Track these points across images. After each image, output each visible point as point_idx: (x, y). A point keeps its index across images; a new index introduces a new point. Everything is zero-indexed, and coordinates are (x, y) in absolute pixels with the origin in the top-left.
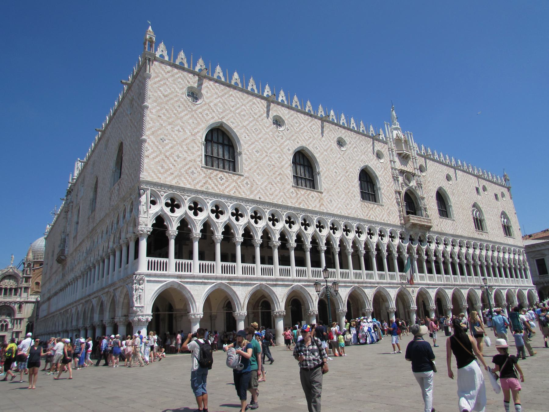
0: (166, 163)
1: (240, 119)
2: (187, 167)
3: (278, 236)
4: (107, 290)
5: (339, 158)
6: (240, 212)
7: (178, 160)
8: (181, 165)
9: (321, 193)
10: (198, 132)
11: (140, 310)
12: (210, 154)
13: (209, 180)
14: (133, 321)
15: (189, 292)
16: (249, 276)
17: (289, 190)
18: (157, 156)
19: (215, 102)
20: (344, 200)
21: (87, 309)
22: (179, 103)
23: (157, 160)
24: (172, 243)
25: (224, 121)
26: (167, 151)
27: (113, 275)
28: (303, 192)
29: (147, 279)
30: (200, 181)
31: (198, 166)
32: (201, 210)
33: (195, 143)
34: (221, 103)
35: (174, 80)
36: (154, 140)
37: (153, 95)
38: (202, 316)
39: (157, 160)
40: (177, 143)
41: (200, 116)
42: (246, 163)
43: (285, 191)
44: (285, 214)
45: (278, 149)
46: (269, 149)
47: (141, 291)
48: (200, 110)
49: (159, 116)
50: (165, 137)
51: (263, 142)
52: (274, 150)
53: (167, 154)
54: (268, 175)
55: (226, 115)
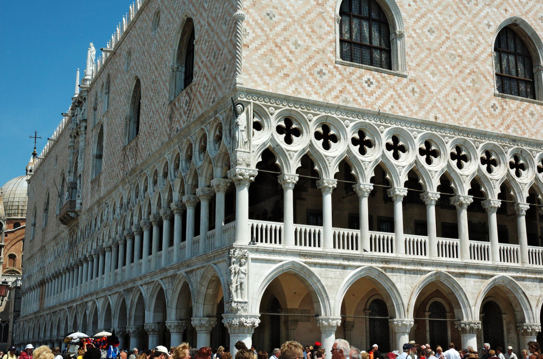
0: (276, 56)
3: (467, 187)
4: (171, 272)
6: (367, 138)
7: (297, 51)
8: (301, 60)
11: (242, 307)
12: (347, 37)
14: (231, 325)
15: (319, 281)
16: (416, 256)
17: (489, 101)
18: (262, 44)
21: (128, 303)
23: (261, 52)
24: (289, 196)
26: (278, 35)
27: (182, 248)
29: (252, 256)
30: (334, 88)
31: (330, 60)
32: (335, 139)
33: (324, 18)
36: (257, 17)
38: (340, 322)
39: (261, 52)
40: (294, 21)
43: (482, 103)
44: (481, 145)
45: (470, 25)
46: (451, 26)
47: (243, 275)
50: (275, 11)
51: (440, 13)
52: (462, 27)
53: (279, 41)
54: (450, 75)
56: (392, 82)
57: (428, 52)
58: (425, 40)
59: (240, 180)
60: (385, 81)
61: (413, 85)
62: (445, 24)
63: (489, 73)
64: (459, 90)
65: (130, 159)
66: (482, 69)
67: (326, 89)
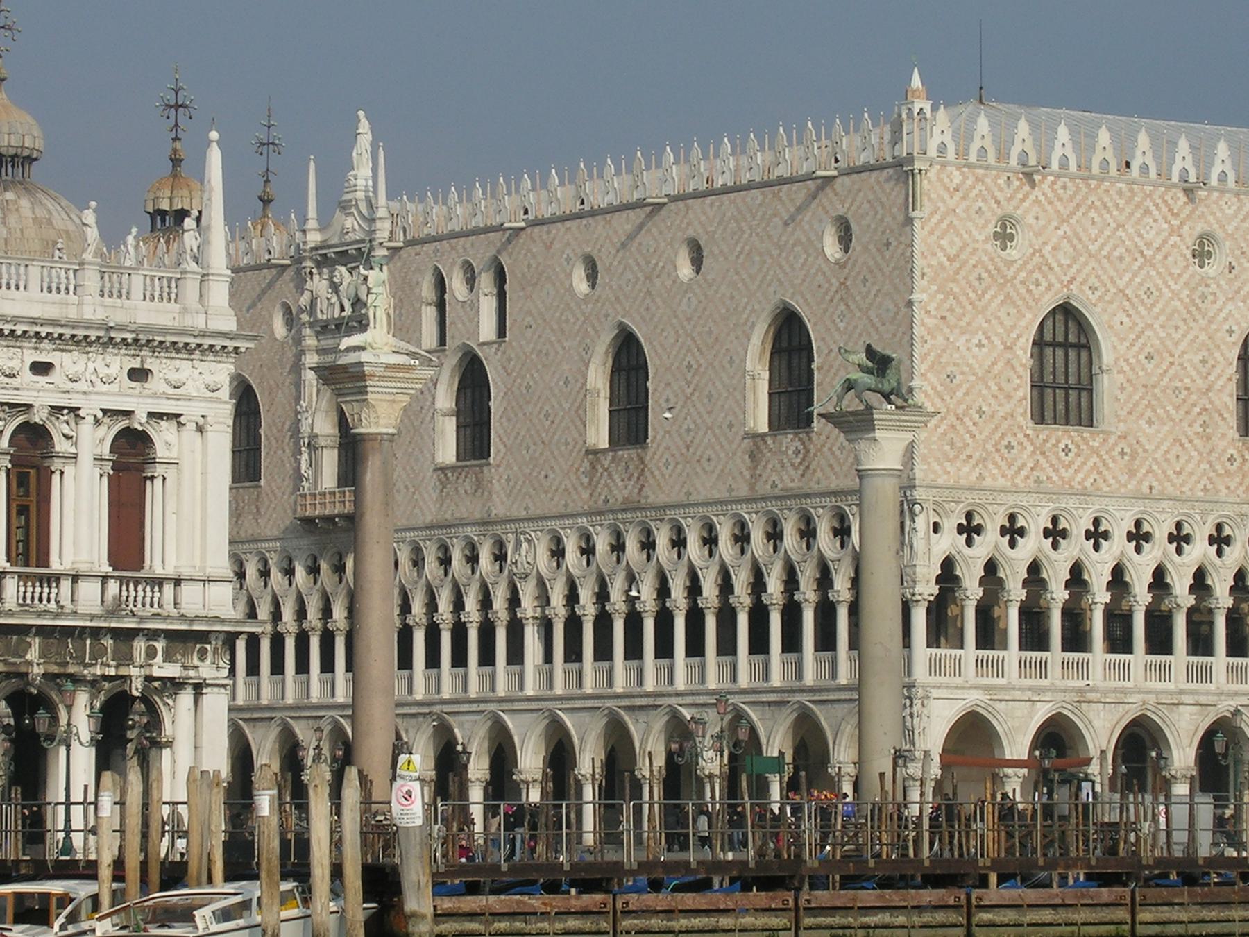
1: (1112, 273)
10: (1019, 337)
13: (1040, 458)
19: (1054, 240)
22: (979, 270)
23: (940, 430)
26: (959, 403)
29: (935, 693)
30: (1024, 465)
31: (1021, 427)
33: (1013, 368)
35: (967, 210)
36: (936, 383)
37: (929, 266)
39: (940, 430)
40: (979, 379)
41: (1023, 291)
42: (1122, 397)
45: (1203, 337)
46: (1177, 344)
48: (1023, 274)
49: (942, 318)
51: (1162, 327)
52: (1193, 341)
53: (960, 411)
54: (1173, 420)
55: (1079, 271)
56: (1096, 444)
57: (1144, 390)
58: (1141, 373)
59: (918, 601)
60: (1087, 444)
61: (1122, 444)
62: (1169, 343)
64: (1184, 441)
65: (616, 477)
66: (1217, 403)
67: (1015, 468)
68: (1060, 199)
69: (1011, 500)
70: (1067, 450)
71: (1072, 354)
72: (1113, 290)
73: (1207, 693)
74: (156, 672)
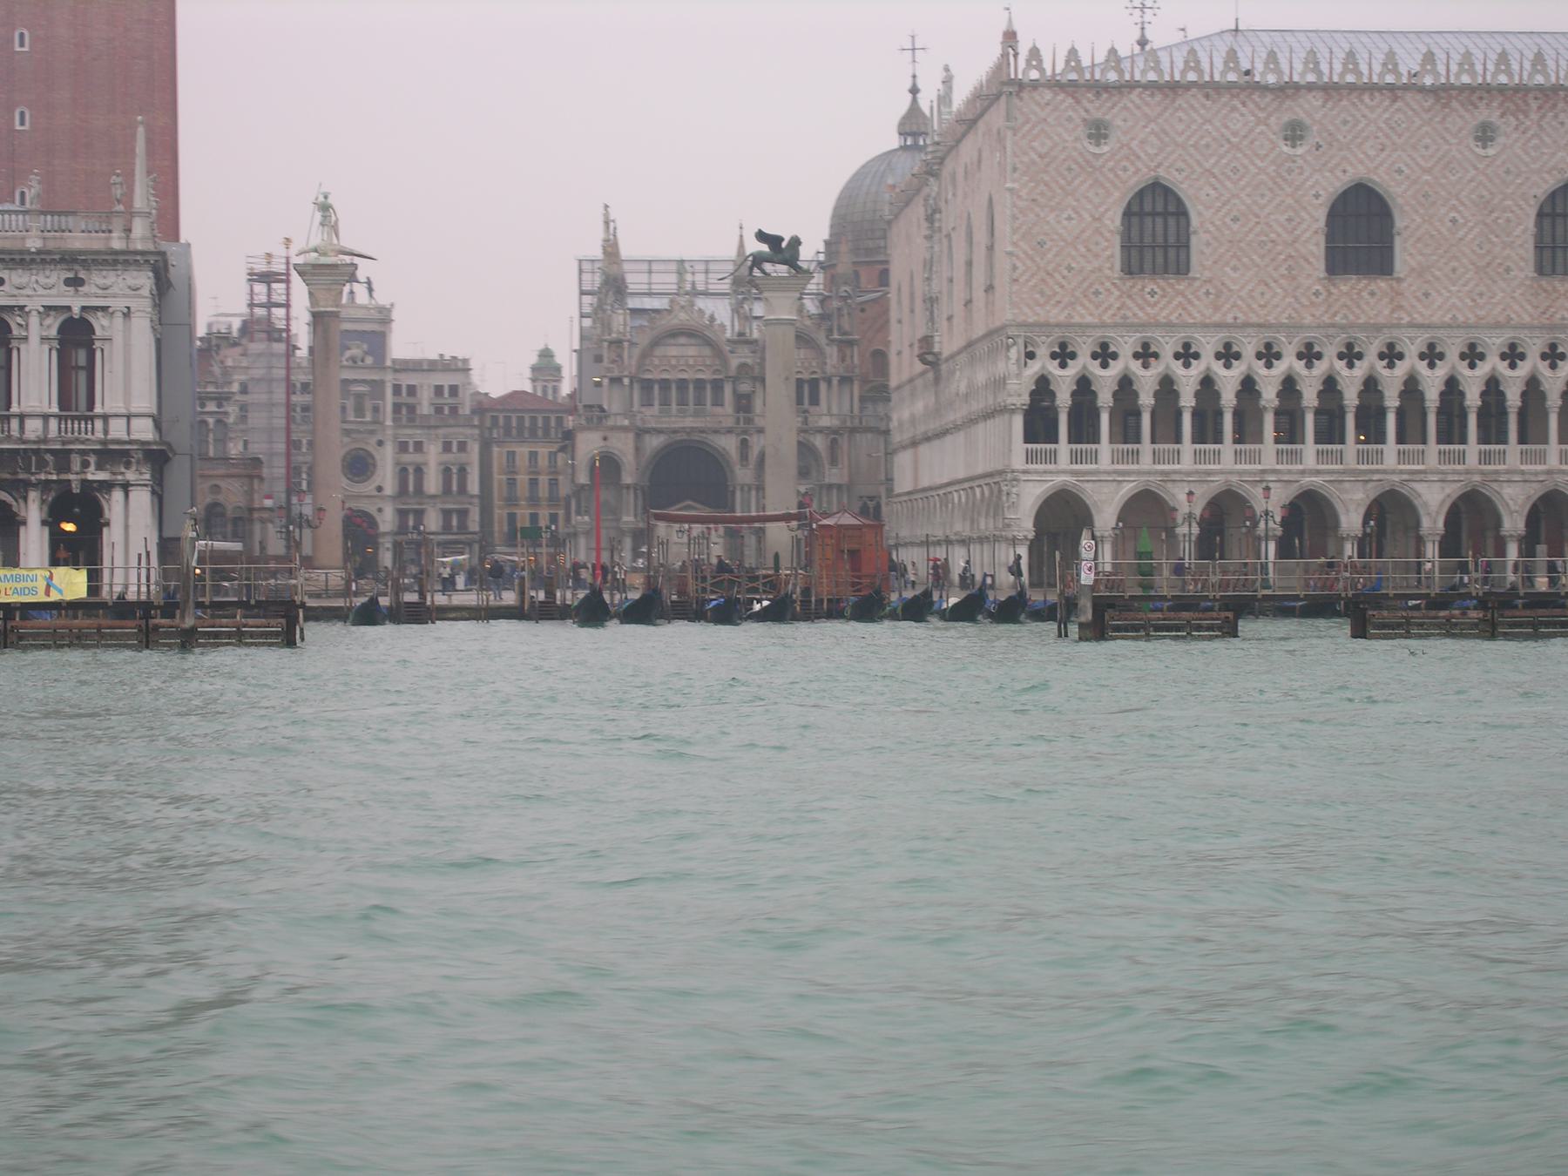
2: (1085, 285)
5: (1471, 181)
9: (1399, 280)
10: (1107, 210)
18: (1032, 276)
20: (1471, 284)
25: (1161, 172)
28: (1344, 288)
30: (1110, 306)
31: (1108, 278)
34: (1156, 135)
41: (1111, 176)
42: (1207, 251)
45: (1290, 201)
46: (1262, 208)
48: (1111, 164)
53: (1050, 268)
60: (1172, 286)
61: (1208, 286)
63: (1312, 254)
64: (1270, 281)
68: (1147, 104)
69: (1098, 333)
70: (1152, 294)
71: (1172, 221)
72: (1199, 170)
73: (1290, 472)
74: (90, 477)
